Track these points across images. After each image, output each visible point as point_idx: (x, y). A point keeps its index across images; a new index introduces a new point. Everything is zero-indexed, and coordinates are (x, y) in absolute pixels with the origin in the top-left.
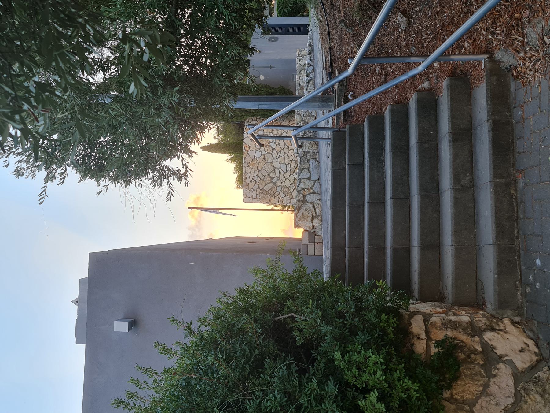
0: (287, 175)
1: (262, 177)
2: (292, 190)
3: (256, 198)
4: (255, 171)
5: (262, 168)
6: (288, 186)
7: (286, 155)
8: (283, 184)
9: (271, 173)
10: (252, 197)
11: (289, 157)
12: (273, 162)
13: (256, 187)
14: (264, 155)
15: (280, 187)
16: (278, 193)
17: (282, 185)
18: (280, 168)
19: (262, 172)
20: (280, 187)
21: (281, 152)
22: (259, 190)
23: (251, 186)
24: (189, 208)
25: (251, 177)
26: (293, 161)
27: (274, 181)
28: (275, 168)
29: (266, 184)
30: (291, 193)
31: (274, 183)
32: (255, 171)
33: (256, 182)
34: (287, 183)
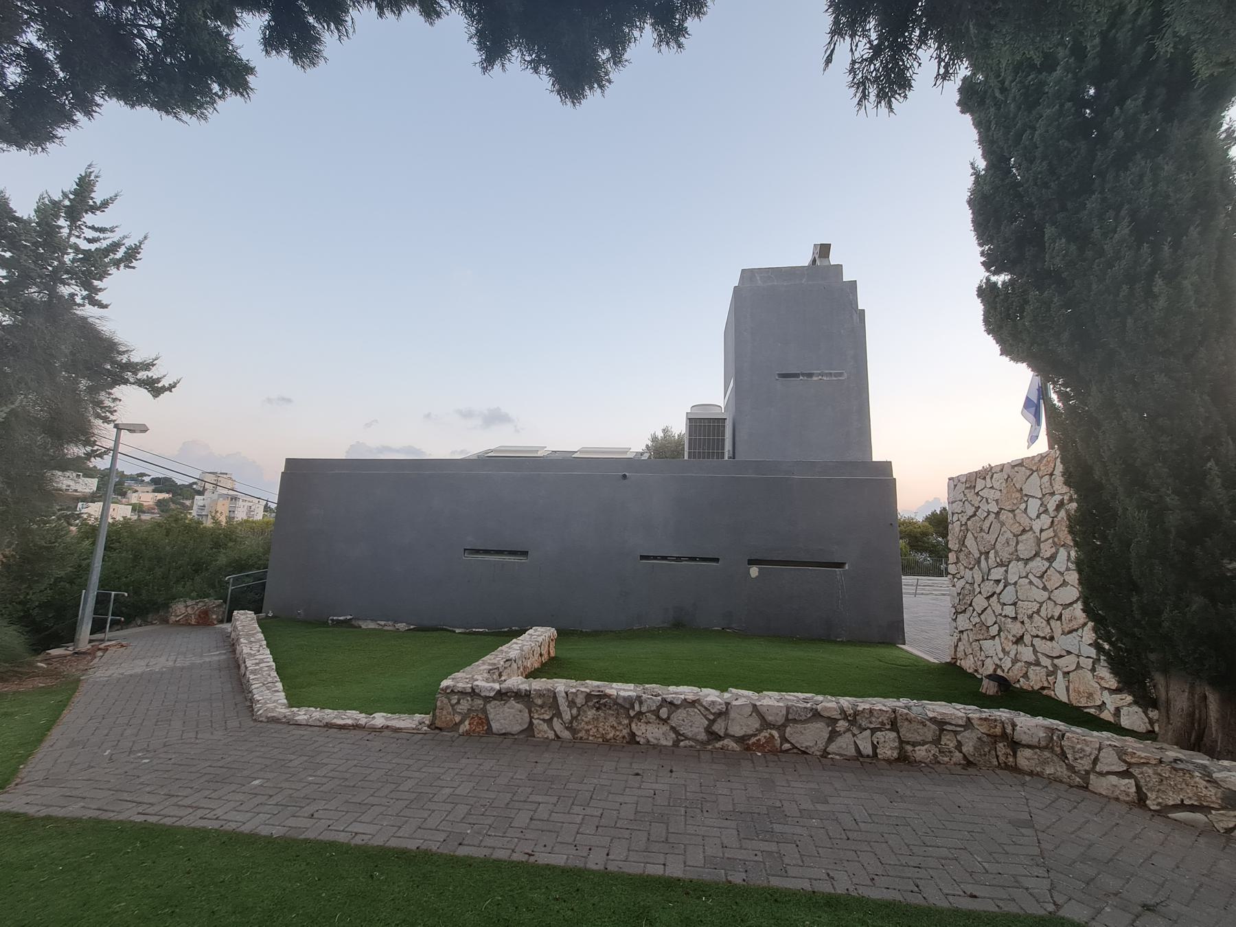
11: (1030, 617)
12: (1018, 559)
13: (970, 511)
17: (976, 585)
19: (996, 526)
21: (1045, 589)
23: (971, 495)
34: (980, 603)
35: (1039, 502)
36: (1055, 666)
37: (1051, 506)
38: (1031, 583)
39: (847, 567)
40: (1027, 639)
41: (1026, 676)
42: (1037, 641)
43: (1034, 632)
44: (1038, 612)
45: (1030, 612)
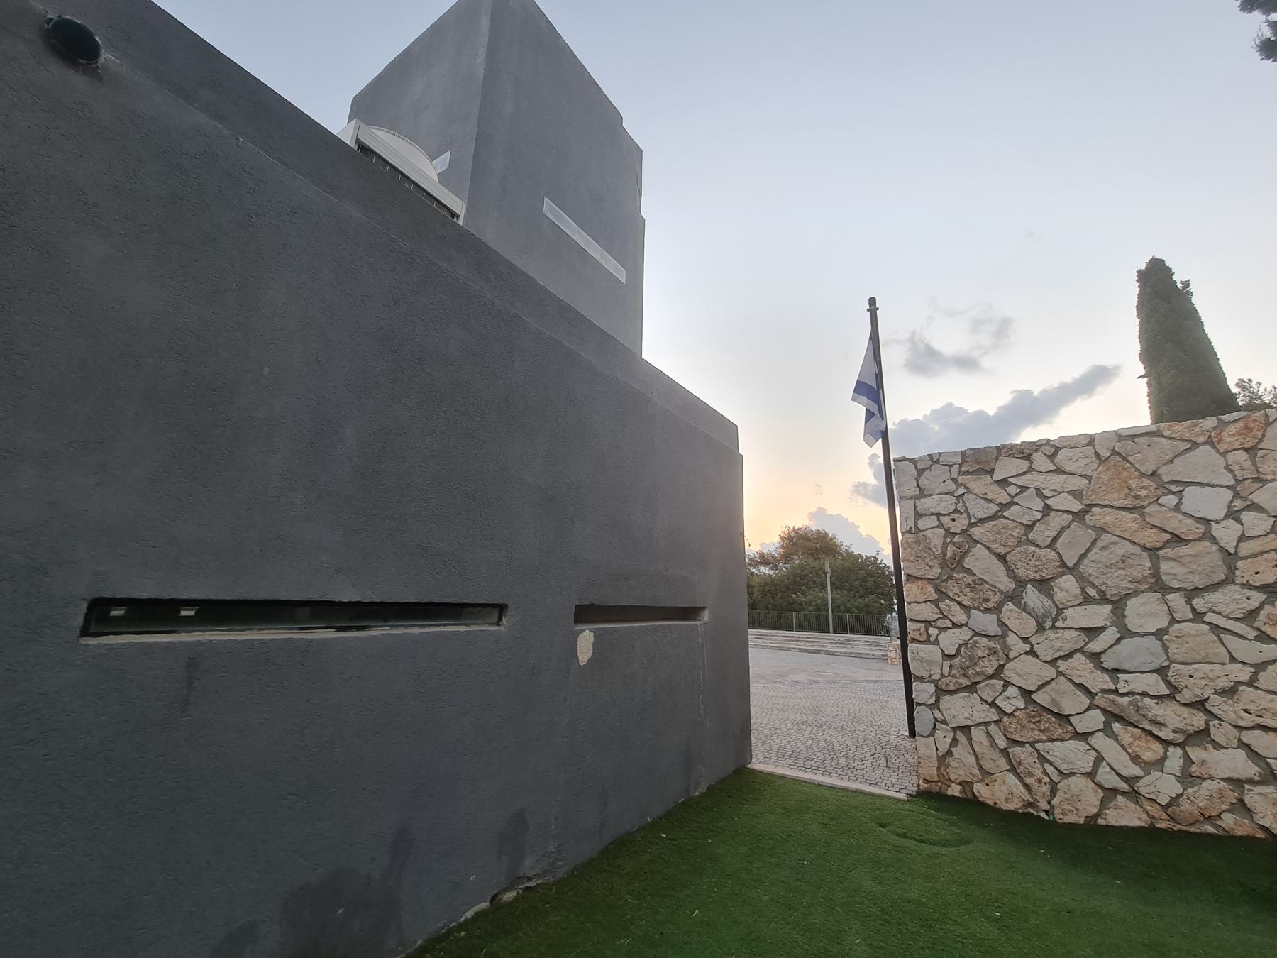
0: (1080, 667)
1: (1042, 534)
2: (986, 691)
3: (918, 515)
4: (1077, 494)
5: (1101, 530)
6: (1008, 673)
7: (1245, 674)
8: (1016, 646)
9: (1083, 580)
10: (922, 493)
11: (1229, 692)
12: (1161, 588)
14: (1208, 536)
15: (993, 629)
16: (960, 617)
17: (1012, 639)
18: (1126, 633)
20: (993, 629)
22: (962, 523)
23: (979, 485)
24: (872, 301)
25: (1031, 480)
26: (1198, 720)
28: (1118, 604)
29: (1002, 558)
30: (971, 688)
31: (1015, 597)
32: (1077, 494)
33: (1004, 506)
34: (1026, 671)
35: (1230, 494)
38: (1215, 628)
39: (706, 616)
41: (1241, 807)
42: (1248, 737)
43: (1248, 720)
44: (1252, 683)
45: (1225, 683)
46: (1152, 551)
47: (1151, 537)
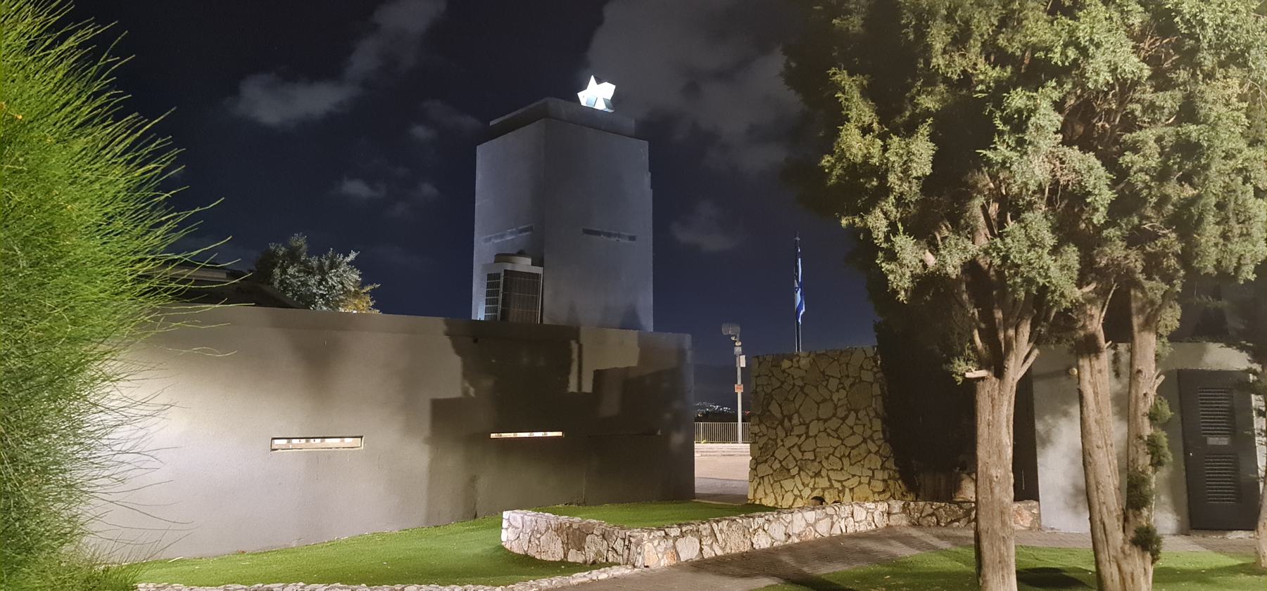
4: (802, 378)
12: (819, 419)
18: (807, 437)
21: (838, 438)
27: (786, 423)
29: (780, 406)
32: (802, 378)
36: (843, 487)
37: (848, 383)
38: (829, 435)
40: (824, 473)
42: (831, 474)
46: (818, 404)
47: (819, 399)
